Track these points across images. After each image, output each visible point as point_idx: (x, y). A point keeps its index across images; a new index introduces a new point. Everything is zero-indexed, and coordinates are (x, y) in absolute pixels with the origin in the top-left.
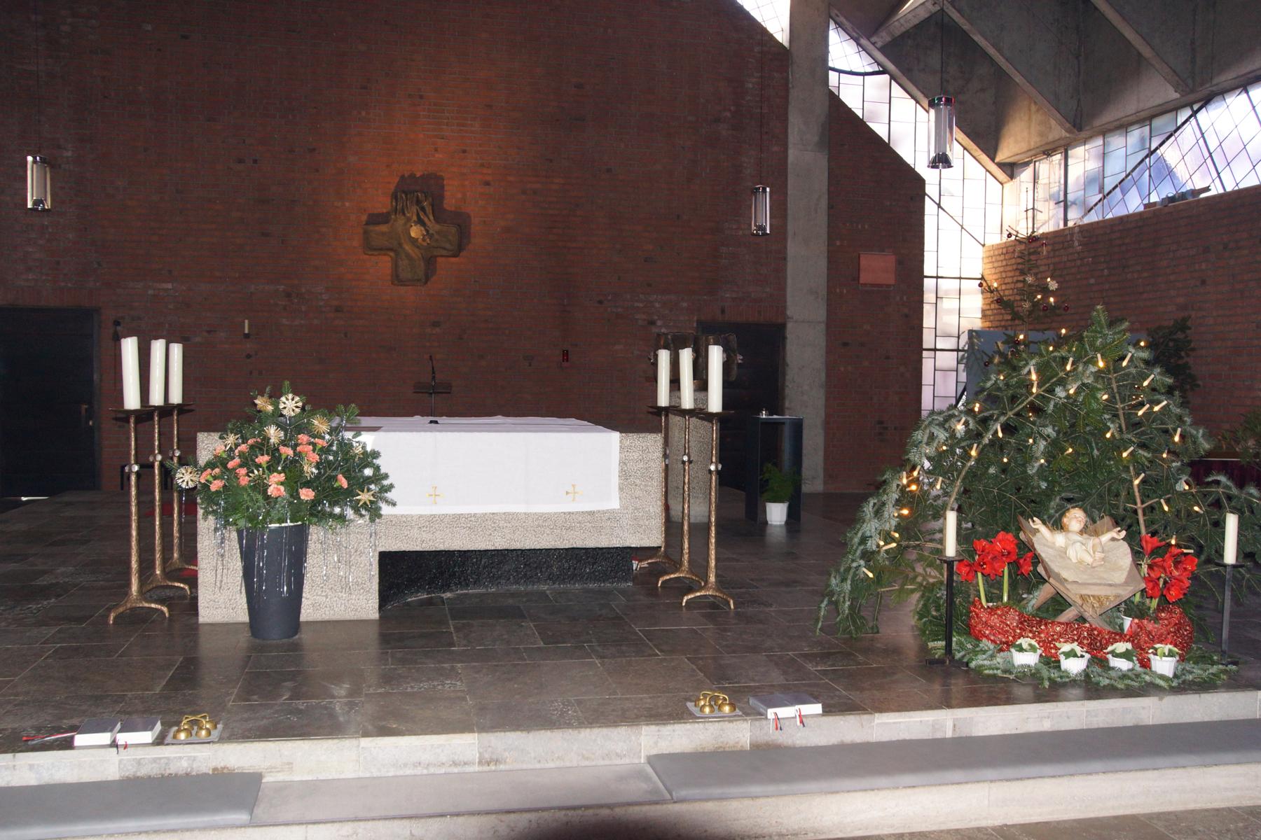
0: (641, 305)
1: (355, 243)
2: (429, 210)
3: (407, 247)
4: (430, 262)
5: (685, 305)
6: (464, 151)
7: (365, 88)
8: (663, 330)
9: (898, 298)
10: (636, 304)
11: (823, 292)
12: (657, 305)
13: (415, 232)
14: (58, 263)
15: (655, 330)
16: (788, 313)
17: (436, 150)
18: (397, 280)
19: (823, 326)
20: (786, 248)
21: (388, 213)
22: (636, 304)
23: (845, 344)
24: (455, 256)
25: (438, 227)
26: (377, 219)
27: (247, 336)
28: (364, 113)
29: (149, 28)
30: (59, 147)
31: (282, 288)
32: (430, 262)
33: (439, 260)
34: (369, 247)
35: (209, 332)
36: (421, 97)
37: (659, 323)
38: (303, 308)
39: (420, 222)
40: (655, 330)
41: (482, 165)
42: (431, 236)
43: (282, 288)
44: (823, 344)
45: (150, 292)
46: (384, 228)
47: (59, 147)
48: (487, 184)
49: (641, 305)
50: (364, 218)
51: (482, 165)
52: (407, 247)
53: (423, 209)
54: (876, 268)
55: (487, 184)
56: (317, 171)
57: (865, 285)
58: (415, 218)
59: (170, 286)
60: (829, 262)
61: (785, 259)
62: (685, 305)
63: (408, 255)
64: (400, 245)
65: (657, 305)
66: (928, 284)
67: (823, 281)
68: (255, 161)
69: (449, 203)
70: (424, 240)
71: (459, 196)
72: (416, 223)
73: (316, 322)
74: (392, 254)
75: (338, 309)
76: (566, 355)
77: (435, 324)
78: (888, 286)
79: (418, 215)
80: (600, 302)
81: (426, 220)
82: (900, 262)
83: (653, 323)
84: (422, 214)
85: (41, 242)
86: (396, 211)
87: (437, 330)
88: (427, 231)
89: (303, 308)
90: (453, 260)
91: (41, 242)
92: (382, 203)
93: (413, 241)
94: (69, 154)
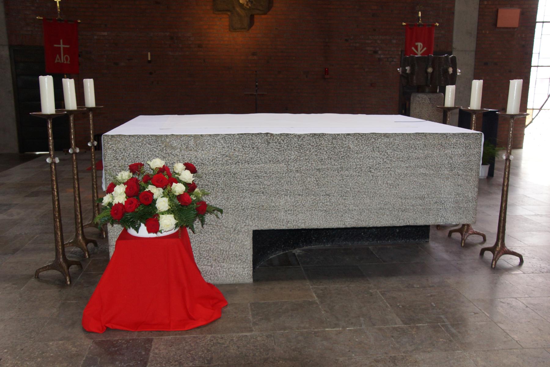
0: (370, 42)
3: (238, 9)
5: (394, 41)
8: (382, 56)
9: (519, 36)
10: (367, 41)
11: (475, 32)
12: (379, 42)
15: (377, 56)
16: (454, 46)
18: (232, 28)
19: (473, 53)
20: (454, 6)
22: (367, 41)
23: (486, 64)
24: (265, 14)
27: (149, 62)
31: (168, 34)
32: (252, 17)
33: (255, 16)
37: (380, 52)
40: (377, 56)
43: (168, 34)
44: (473, 64)
45: (96, 37)
49: (370, 42)
52: (238, 9)
54: (508, 17)
57: (500, 28)
59: (106, 34)
60: (479, 15)
61: (453, 13)
62: (394, 41)
65: (379, 42)
66: (538, 26)
67: (475, 26)
74: (229, 13)
75: (200, 46)
76: (326, 72)
77: (254, 54)
78: (514, 28)
80: (346, 40)
82: (522, 14)
83: (376, 52)
85: (33, 8)
90: (263, 16)
91: (33, 8)
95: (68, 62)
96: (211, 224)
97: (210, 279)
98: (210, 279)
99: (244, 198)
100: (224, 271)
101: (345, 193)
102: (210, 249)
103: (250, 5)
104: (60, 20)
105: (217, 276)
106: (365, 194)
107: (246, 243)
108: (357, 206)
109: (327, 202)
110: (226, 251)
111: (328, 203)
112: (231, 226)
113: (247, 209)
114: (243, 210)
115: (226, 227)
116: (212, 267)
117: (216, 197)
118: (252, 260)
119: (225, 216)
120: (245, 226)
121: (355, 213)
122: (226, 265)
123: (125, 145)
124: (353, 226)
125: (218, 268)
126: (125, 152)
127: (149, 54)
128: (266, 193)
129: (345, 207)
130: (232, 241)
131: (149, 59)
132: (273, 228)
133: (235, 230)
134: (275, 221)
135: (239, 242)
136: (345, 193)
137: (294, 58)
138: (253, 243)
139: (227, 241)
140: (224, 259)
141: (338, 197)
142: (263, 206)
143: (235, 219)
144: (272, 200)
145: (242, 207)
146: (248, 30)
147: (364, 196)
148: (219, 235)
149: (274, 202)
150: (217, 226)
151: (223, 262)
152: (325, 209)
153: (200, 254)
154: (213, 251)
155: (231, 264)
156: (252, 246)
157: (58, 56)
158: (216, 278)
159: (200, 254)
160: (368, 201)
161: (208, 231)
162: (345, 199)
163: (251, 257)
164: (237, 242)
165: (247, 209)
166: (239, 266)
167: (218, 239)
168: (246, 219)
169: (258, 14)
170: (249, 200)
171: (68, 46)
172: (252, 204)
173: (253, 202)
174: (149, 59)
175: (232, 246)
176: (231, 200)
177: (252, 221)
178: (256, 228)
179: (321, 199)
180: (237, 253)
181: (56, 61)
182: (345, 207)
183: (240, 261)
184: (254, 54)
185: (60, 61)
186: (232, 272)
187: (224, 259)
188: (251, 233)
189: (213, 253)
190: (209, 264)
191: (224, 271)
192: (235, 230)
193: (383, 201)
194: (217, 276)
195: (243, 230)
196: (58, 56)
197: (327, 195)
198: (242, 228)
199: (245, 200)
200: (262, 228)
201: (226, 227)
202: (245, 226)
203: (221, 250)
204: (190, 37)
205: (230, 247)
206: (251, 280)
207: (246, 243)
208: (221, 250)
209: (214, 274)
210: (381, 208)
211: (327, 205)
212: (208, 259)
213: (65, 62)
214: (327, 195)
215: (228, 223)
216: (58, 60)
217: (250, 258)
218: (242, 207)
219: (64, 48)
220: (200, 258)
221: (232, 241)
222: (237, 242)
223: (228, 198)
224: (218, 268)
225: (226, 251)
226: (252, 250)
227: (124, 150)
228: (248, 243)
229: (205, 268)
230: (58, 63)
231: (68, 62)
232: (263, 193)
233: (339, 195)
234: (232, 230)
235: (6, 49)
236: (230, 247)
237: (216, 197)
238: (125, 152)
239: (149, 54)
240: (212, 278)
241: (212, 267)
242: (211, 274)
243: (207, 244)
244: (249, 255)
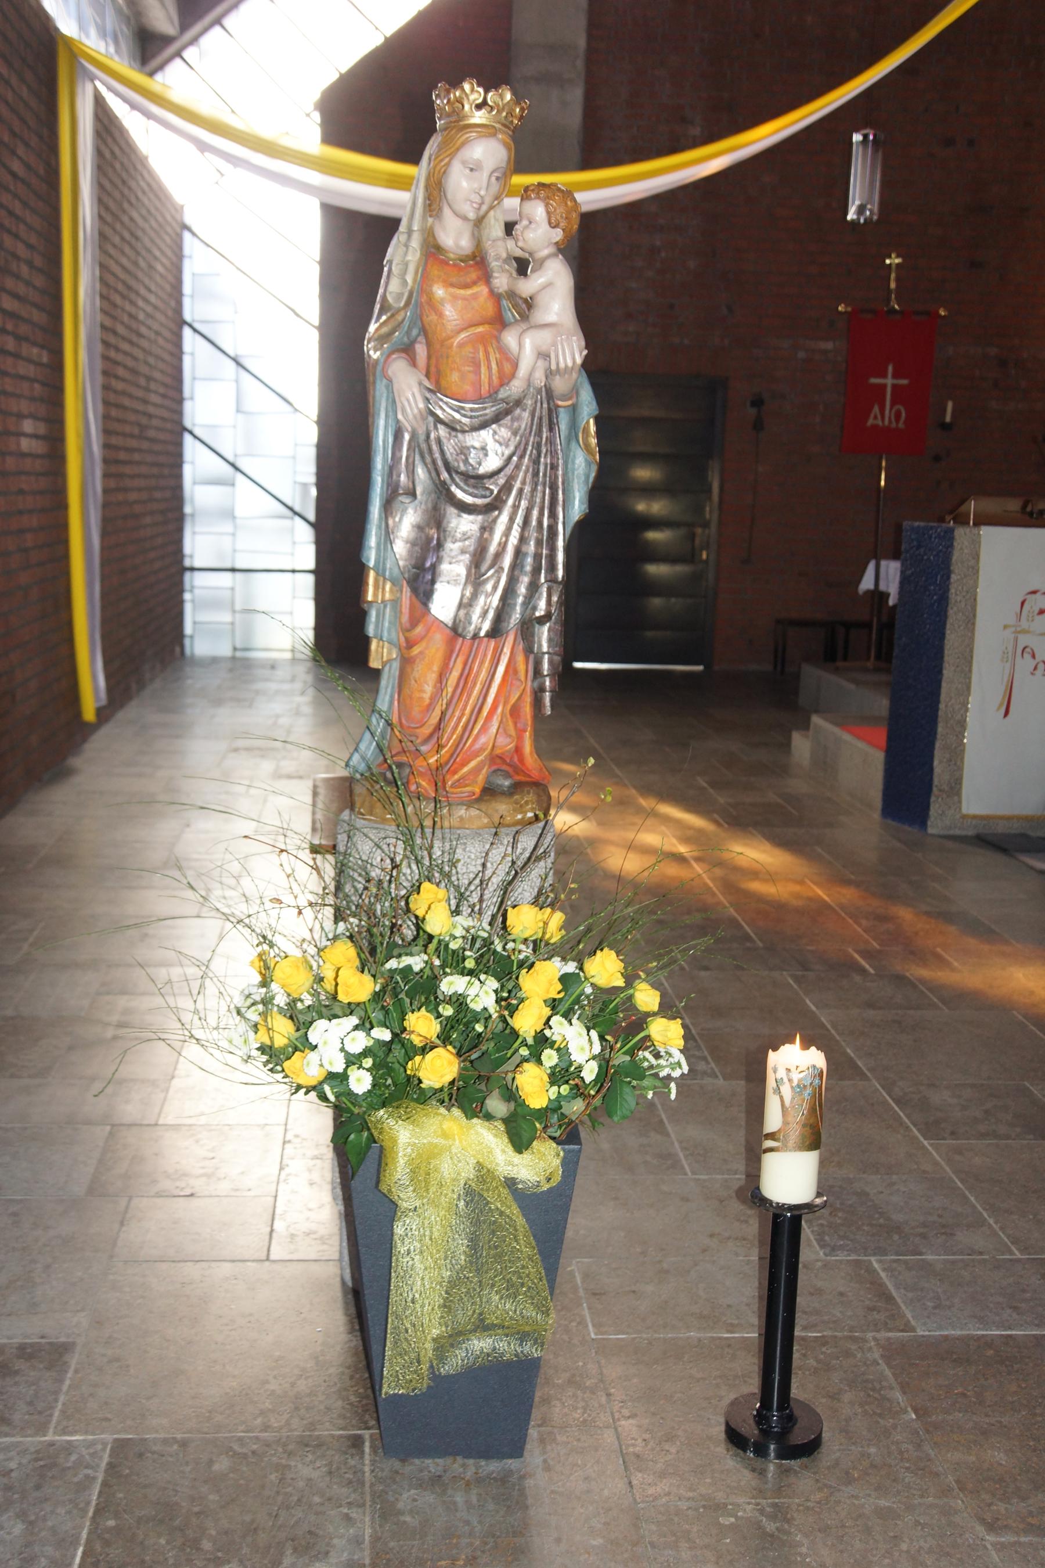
14: (672, 307)
27: (944, 427)
31: (993, 351)
45: (801, 355)
68: (971, 143)
95: (901, 425)
127: (950, 405)
131: (948, 419)
157: (876, 409)
171: (905, 382)
174: (948, 419)
181: (871, 422)
185: (880, 423)
196: (876, 409)
213: (894, 425)
216: (875, 418)
219: (894, 386)
230: (875, 427)
231: (901, 425)
239: (950, 405)
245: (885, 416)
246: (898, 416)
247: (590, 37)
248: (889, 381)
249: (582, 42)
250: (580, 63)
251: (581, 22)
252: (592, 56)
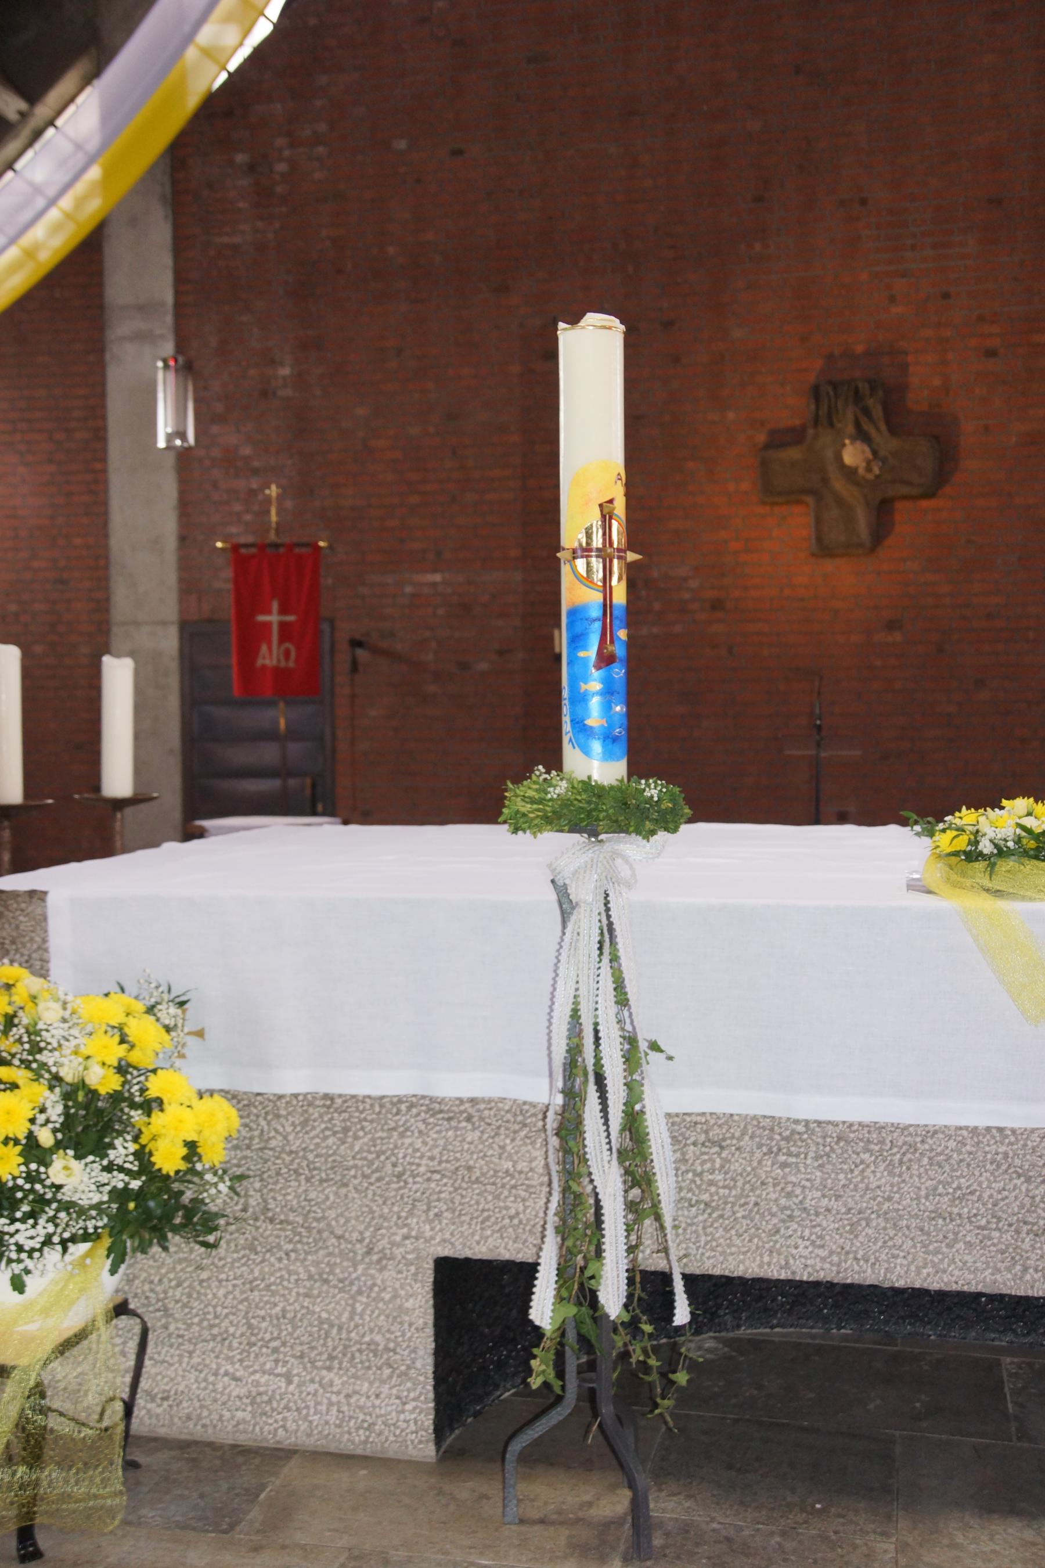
1: (745, 486)
2: (878, 412)
3: (839, 485)
4: (883, 511)
6: (946, 296)
7: (759, 199)
13: (852, 455)
17: (892, 299)
21: (804, 428)
25: (894, 444)
26: (780, 439)
28: (758, 246)
29: (402, 145)
30: (273, 362)
32: (883, 511)
33: (899, 505)
34: (774, 491)
35: (500, 653)
36: (864, 202)
38: (657, 606)
39: (862, 435)
41: (981, 319)
42: (884, 460)
45: (408, 589)
46: (794, 453)
47: (273, 362)
48: (991, 353)
50: (761, 438)
51: (981, 319)
52: (839, 485)
53: (867, 412)
55: (991, 353)
56: (677, 360)
58: (851, 429)
59: (437, 577)
63: (840, 502)
64: (825, 481)
69: (917, 399)
70: (869, 469)
71: (937, 382)
72: (853, 439)
73: (678, 629)
75: (717, 605)
77: (892, 625)
79: (858, 424)
81: (873, 432)
84: (867, 426)
85: (248, 517)
86: (816, 421)
87: (898, 636)
88: (875, 453)
89: (657, 606)
90: (924, 503)
91: (248, 517)
92: (789, 407)
93: (849, 473)
94: (285, 371)
96: (289, 1223)
97: (283, 1427)
98: (283, 1427)
99: (402, 1135)
100: (331, 1404)
101: (787, 1139)
102: (284, 1310)
103: (876, 471)
104: (276, 546)
105: (305, 1418)
106: (866, 1150)
107: (409, 1304)
108: (838, 1197)
109: (712, 1171)
110: (340, 1328)
111: (718, 1177)
112: (355, 1236)
113: (414, 1176)
114: (399, 1176)
115: (339, 1238)
116: (289, 1382)
117: (305, 1123)
118: (430, 1369)
119: (336, 1194)
120: (406, 1237)
121: (828, 1223)
122: (337, 1381)
123: (17, 927)
124: (821, 1276)
125: (312, 1388)
126: (17, 950)
128: (482, 1119)
129: (789, 1195)
130: (360, 1292)
132: (506, 1256)
133: (369, 1252)
134: (515, 1228)
135: (387, 1296)
136: (787, 1139)
137: (1031, 635)
138: (436, 1306)
139: (341, 1290)
140: (331, 1358)
141: (758, 1155)
142: (469, 1169)
143: (371, 1212)
144: (503, 1148)
145: (394, 1165)
146: (873, 550)
147: (865, 1156)
148: (316, 1263)
149: (510, 1157)
150: (309, 1229)
151: (329, 1369)
152: (705, 1197)
153: (250, 1327)
154: (292, 1321)
155: (355, 1377)
156: (430, 1319)
157: (264, 648)
158: (304, 1426)
159: (250, 1327)
160: (879, 1177)
161: (279, 1246)
162: (784, 1165)
163: (430, 1360)
164: (378, 1299)
165: (414, 1176)
166: (385, 1389)
167: (310, 1277)
168: (411, 1213)
169: (905, 498)
170: (418, 1144)
172: (432, 1158)
173: (436, 1152)
175: (359, 1308)
176: (356, 1138)
177: (431, 1222)
178: (446, 1252)
179: (690, 1155)
180: (378, 1338)
181: (260, 662)
182: (789, 1195)
183: (387, 1371)
184: (892, 625)
185: (267, 662)
186: (361, 1408)
187: (331, 1358)
188: (429, 1267)
189: (295, 1328)
190: (280, 1370)
191: (331, 1404)
192: (369, 1252)
193: (946, 1184)
194: (305, 1418)
195: (398, 1252)
197: (714, 1143)
198: (393, 1244)
199: (407, 1141)
200: (468, 1253)
201: (339, 1238)
202: (406, 1237)
203: (321, 1323)
204: (685, 579)
205: (353, 1313)
206: (429, 1451)
207: (409, 1304)
208: (321, 1322)
209: (298, 1409)
210: (937, 1214)
211: (711, 1183)
212: (275, 1350)
214: (714, 1143)
215: (347, 1221)
217: (425, 1363)
218: (394, 1165)
219: (282, 625)
220: (251, 1344)
221: (360, 1292)
222: (378, 1299)
223: (346, 1130)
224: (312, 1388)
225: (340, 1328)
226: (430, 1331)
227: (13, 942)
228: (418, 1303)
229: (267, 1385)
232: (469, 1119)
233: (760, 1146)
234: (360, 1249)
235: (173, 632)
236: (353, 1313)
237: (305, 1123)
238: (17, 950)
240: (291, 1426)
241: (289, 1382)
242: (287, 1408)
243: (274, 1293)
244: (421, 1353)
245: (270, 656)
246: (287, 654)
247: (178, 293)
248: (274, 618)
249: (169, 298)
250: (169, 319)
251: (167, 279)
252: (179, 307)
